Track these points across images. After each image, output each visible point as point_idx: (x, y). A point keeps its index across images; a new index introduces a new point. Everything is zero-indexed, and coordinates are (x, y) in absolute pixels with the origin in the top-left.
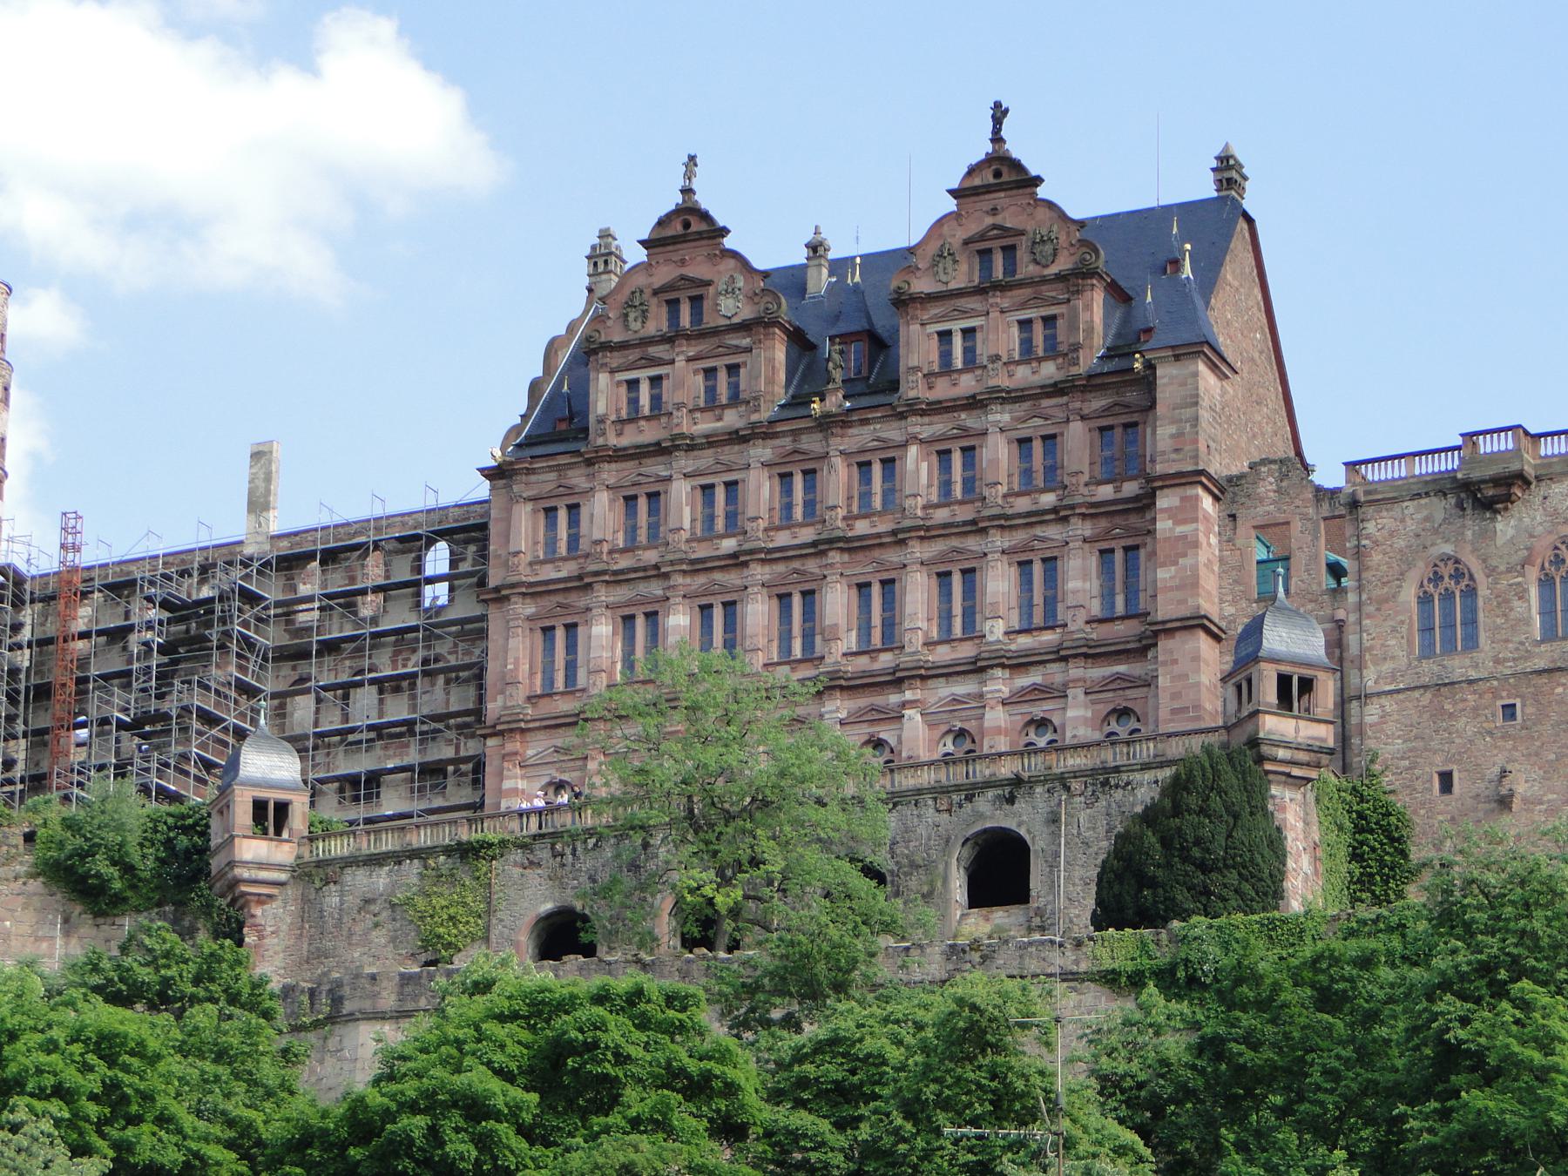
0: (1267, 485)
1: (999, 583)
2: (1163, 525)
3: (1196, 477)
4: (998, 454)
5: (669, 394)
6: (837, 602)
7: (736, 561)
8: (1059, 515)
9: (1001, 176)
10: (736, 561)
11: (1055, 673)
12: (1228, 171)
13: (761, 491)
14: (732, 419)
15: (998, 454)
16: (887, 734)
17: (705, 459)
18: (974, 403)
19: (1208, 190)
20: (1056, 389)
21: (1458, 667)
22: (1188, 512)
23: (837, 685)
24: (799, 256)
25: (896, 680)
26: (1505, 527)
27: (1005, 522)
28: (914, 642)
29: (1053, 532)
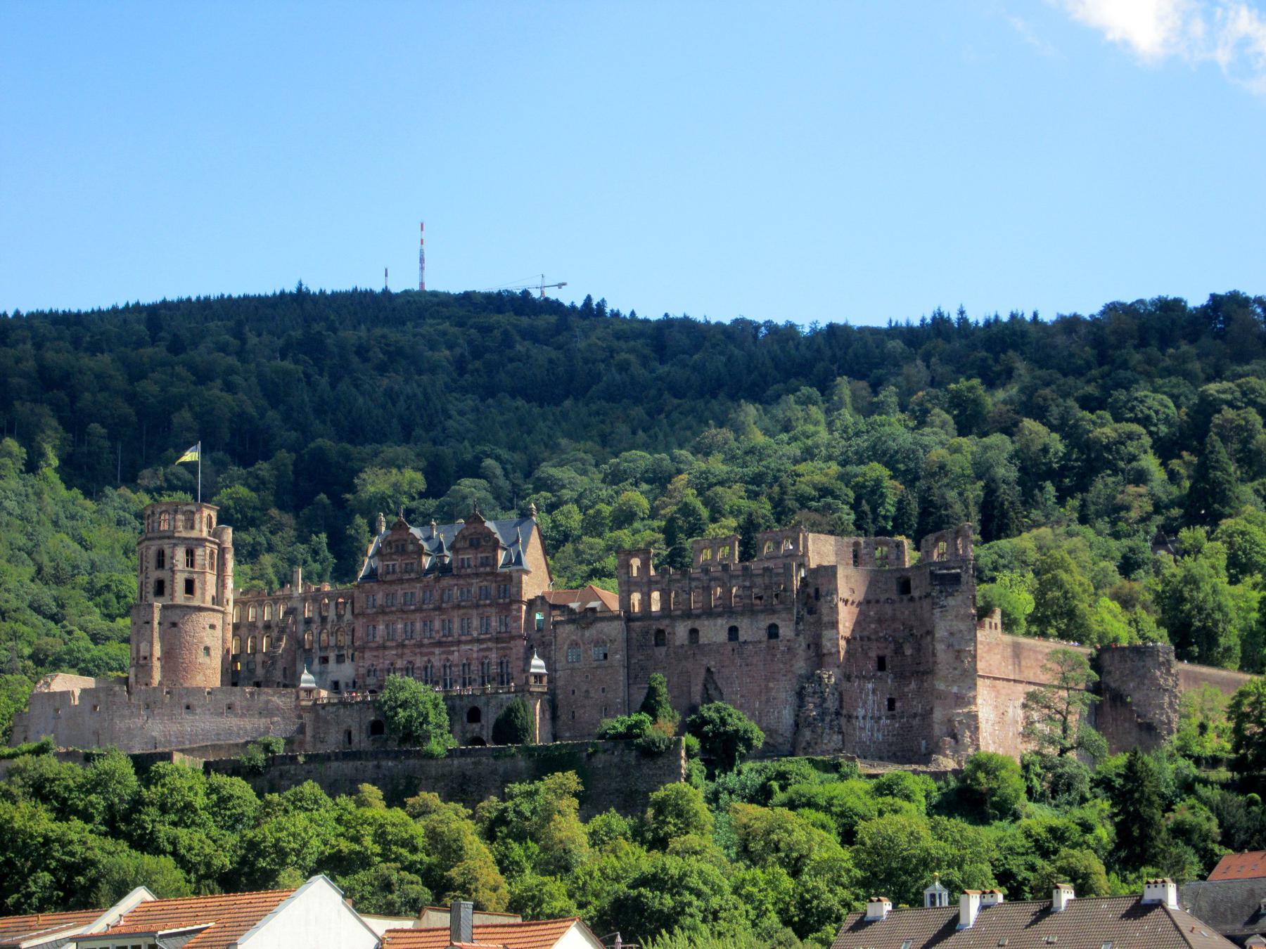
0: (539, 602)
1: (475, 622)
3: (522, 602)
5: (398, 569)
6: (437, 624)
8: (489, 605)
11: (490, 644)
14: (413, 576)
16: (450, 658)
17: (406, 586)
18: (468, 576)
20: (487, 574)
22: (520, 609)
25: (452, 644)
26: (587, 633)
27: (477, 606)
28: (456, 636)
29: (488, 609)
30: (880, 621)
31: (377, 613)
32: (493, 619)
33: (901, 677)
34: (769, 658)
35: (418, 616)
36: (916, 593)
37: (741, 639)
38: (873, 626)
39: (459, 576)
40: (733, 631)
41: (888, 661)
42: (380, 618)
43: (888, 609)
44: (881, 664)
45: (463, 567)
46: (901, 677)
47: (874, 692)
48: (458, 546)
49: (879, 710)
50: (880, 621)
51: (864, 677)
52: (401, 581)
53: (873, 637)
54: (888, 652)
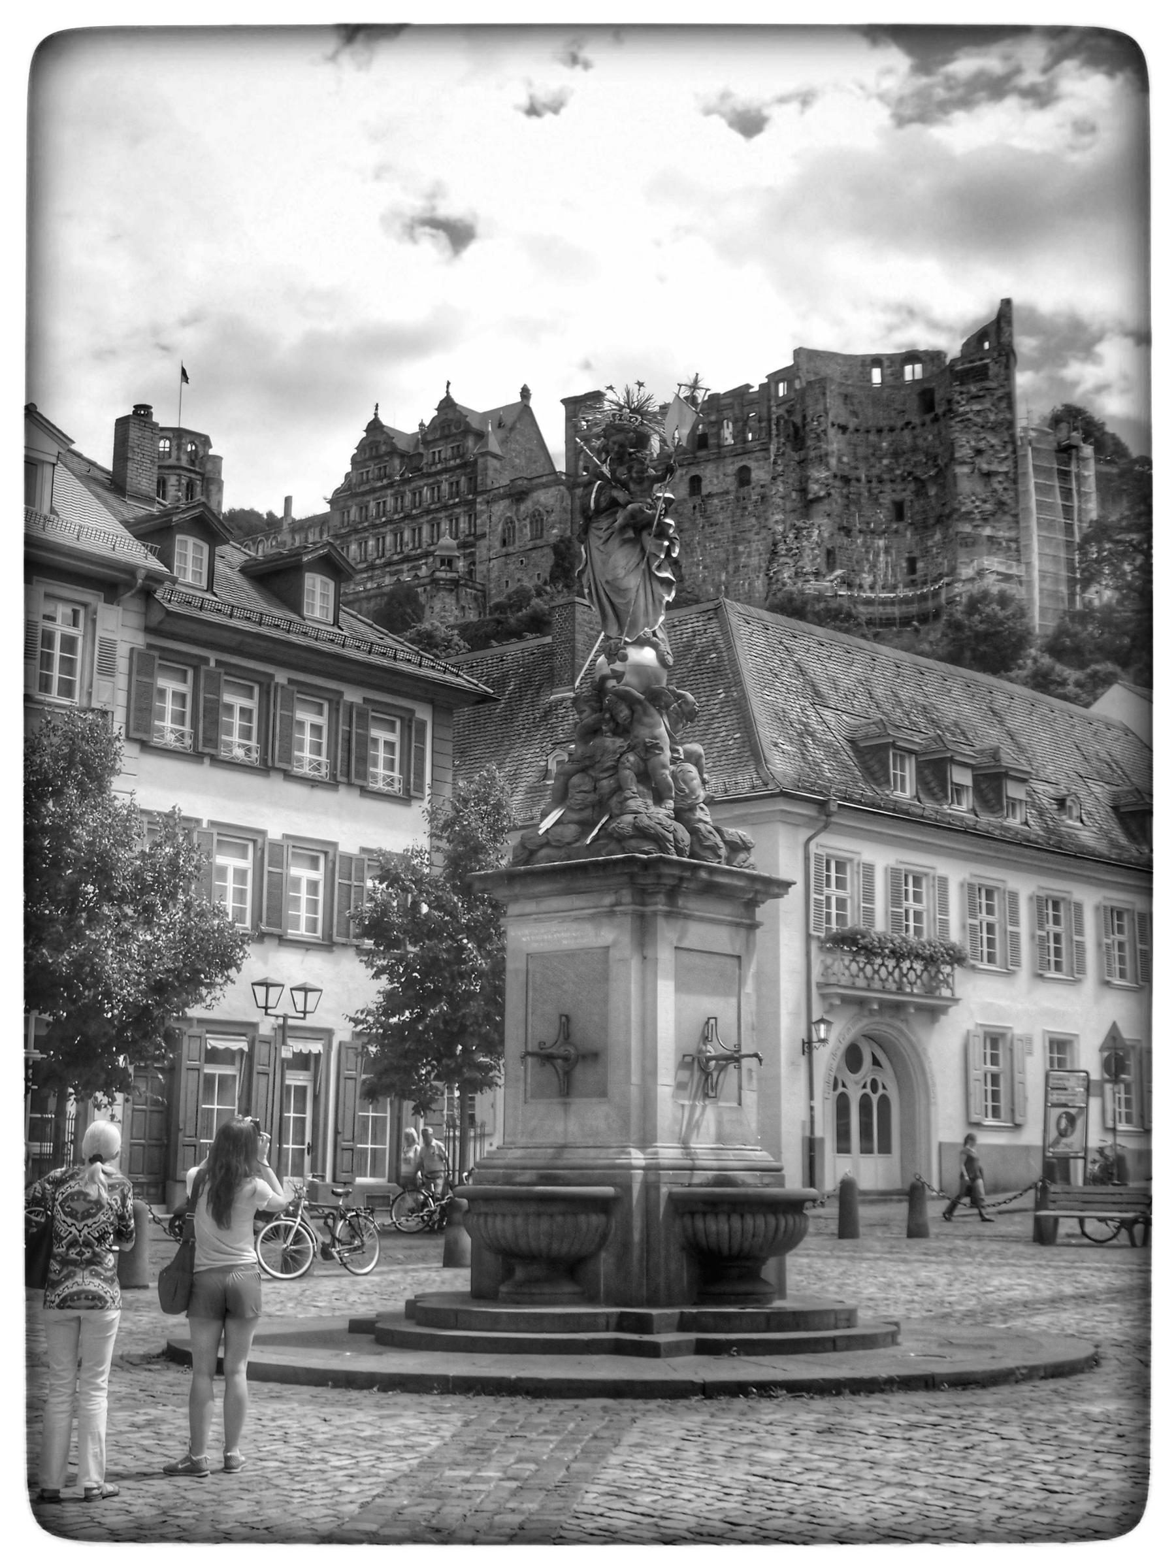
2: (478, 507)
4: (445, 487)
7: (384, 524)
9: (447, 404)
10: (384, 524)
12: (525, 393)
13: (390, 502)
14: (385, 482)
15: (445, 487)
18: (439, 473)
19: (519, 399)
20: (458, 467)
21: (511, 549)
23: (406, 559)
24: (416, 429)
26: (523, 508)
27: (445, 507)
28: (424, 546)
29: (457, 510)
30: (896, 454)
31: (348, 534)
32: (462, 519)
33: (923, 528)
34: (739, 512)
35: (389, 527)
36: (940, 410)
37: (704, 492)
38: (885, 462)
39: (429, 475)
40: (695, 482)
41: (907, 504)
42: (353, 537)
43: (907, 436)
44: (899, 511)
45: (434, 463)
46: (923, 528)
47: (887, 550)
48: (430, 438)
49: (894, 575)
50: (896, 454)
51: (873, 532)
52: (373, 490)
53: (886, 477)
54: (907, 495)
